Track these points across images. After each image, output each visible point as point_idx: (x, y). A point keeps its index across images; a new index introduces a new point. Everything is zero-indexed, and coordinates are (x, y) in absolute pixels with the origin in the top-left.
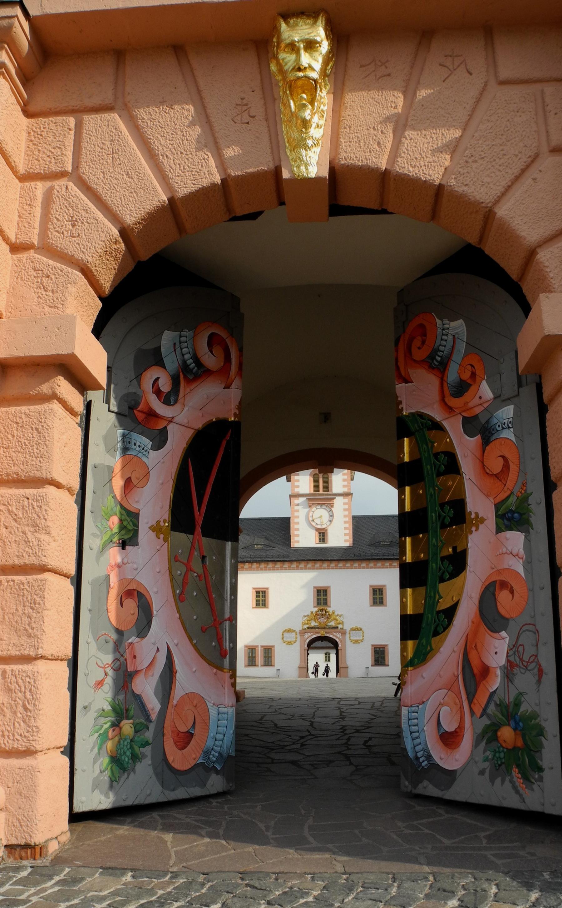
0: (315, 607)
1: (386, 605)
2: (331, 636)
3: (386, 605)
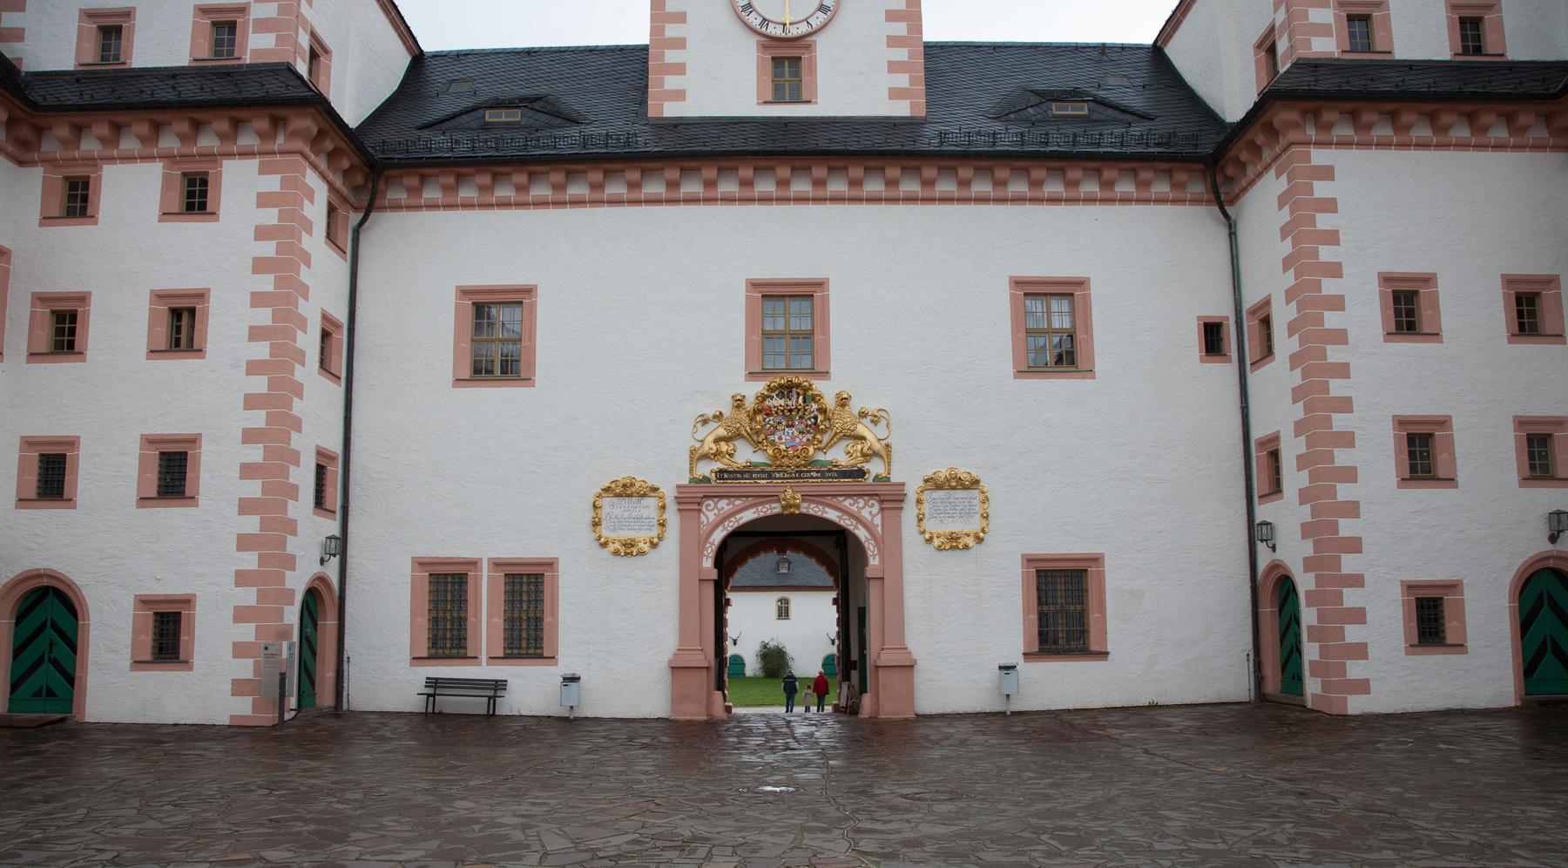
0: (752, 375)
1: (1089, 373)
2: (832, 515)
3: (1089, 373)
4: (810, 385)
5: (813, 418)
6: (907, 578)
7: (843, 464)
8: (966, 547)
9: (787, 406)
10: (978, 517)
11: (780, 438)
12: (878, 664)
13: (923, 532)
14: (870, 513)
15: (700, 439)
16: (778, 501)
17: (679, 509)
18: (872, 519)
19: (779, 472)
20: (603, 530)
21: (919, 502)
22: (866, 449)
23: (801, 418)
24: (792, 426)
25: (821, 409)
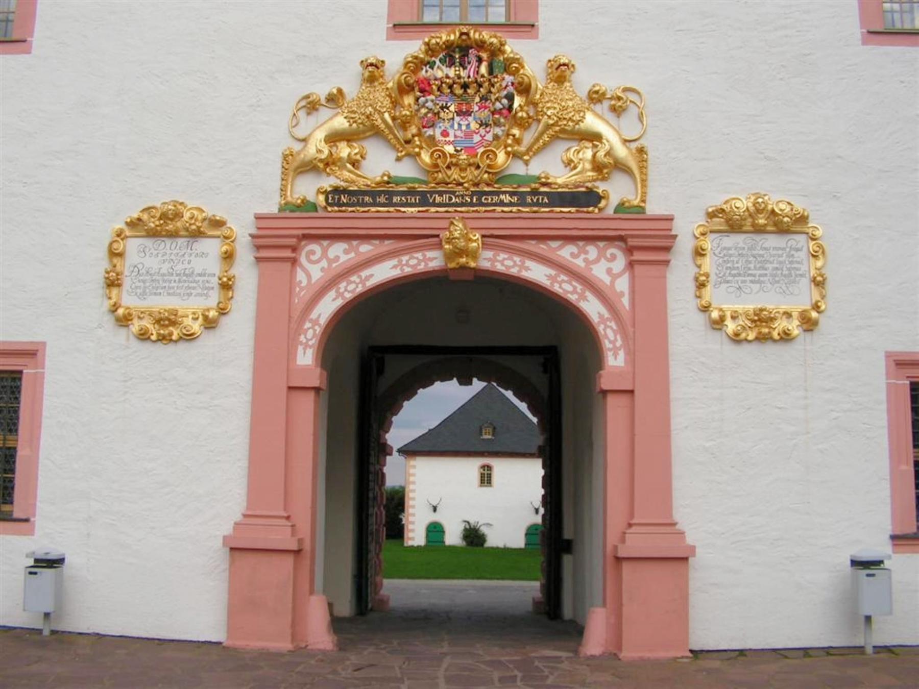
0: (399, 29)
4: (506, 42)
5: (506, 97)
6: (677, 392)
7: (560, 181)
8: (786, 337)
9: (459, 77)
10: (805, 282)
11: (445, 134)
12: (622, 553)
13: (705, 309)
14: (609, 271)
15: (301, 136)
16: (439, 246)
17: (256, 258)
18: (613, 282)
19: (441, 194)
20: (124, 294)
21: (699, 253)
22: (601, 154)
23: (484, 99)
24: (468, 113)
25: (520, 84)
